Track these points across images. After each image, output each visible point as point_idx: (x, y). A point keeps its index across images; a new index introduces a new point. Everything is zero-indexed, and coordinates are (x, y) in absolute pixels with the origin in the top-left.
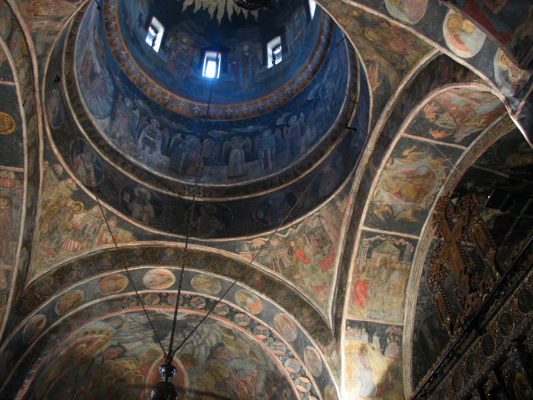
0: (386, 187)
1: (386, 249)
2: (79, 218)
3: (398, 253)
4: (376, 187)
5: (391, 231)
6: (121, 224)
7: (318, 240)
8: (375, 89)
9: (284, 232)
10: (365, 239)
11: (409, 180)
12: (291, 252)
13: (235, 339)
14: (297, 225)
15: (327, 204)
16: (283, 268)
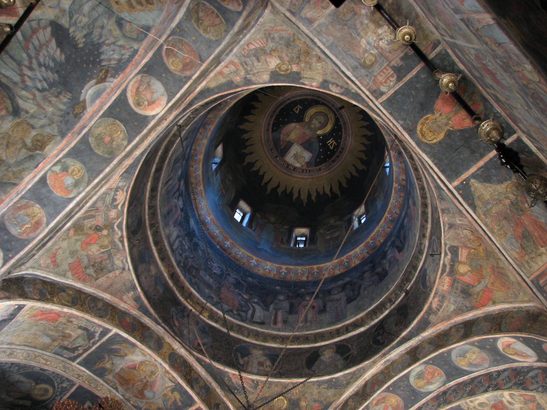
0: (147, 362)
1: (80, 340)
2: (273, 63)
3: (70, 346)
4: (151, 356)
5: (97, 348)
6: (230, 84)
7: (101, 262)
8: (231, 376)
9: (120, 226)
10: (101, 329)
11: (145, 381)
12: (98, 229)
13: (25, 145)
14: (122, 242)
15: (133, 280)
16: (84, 220)
